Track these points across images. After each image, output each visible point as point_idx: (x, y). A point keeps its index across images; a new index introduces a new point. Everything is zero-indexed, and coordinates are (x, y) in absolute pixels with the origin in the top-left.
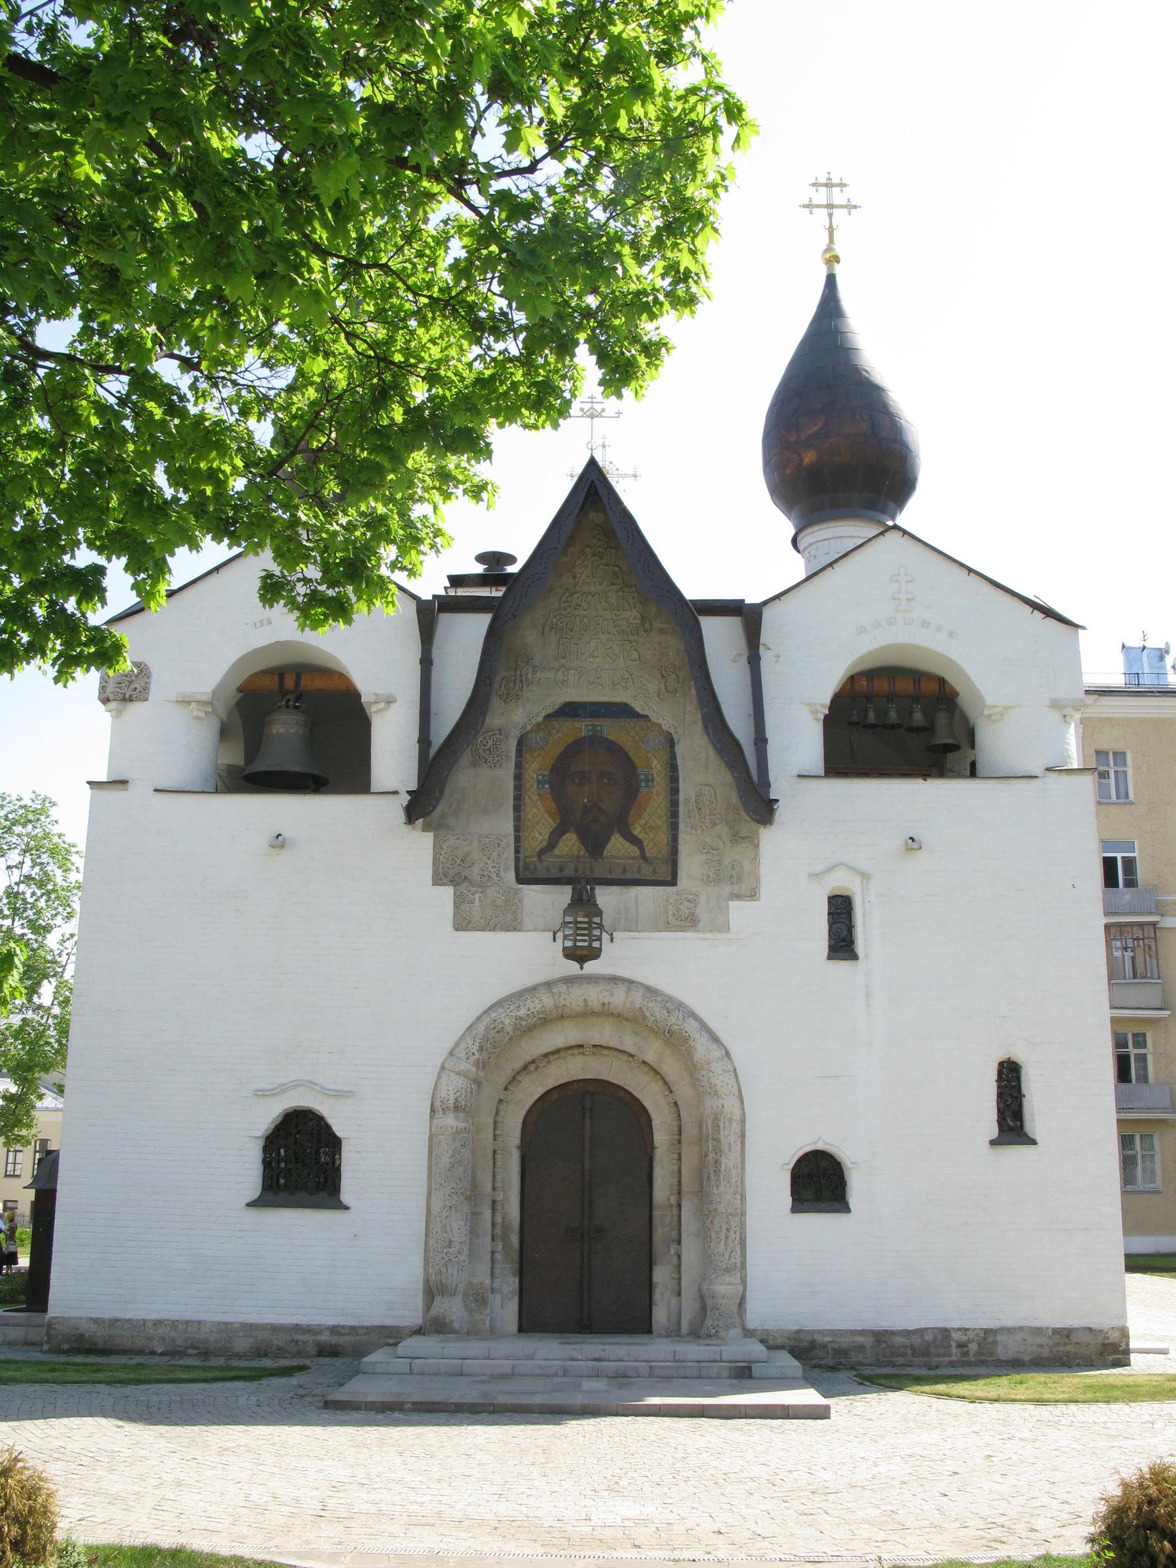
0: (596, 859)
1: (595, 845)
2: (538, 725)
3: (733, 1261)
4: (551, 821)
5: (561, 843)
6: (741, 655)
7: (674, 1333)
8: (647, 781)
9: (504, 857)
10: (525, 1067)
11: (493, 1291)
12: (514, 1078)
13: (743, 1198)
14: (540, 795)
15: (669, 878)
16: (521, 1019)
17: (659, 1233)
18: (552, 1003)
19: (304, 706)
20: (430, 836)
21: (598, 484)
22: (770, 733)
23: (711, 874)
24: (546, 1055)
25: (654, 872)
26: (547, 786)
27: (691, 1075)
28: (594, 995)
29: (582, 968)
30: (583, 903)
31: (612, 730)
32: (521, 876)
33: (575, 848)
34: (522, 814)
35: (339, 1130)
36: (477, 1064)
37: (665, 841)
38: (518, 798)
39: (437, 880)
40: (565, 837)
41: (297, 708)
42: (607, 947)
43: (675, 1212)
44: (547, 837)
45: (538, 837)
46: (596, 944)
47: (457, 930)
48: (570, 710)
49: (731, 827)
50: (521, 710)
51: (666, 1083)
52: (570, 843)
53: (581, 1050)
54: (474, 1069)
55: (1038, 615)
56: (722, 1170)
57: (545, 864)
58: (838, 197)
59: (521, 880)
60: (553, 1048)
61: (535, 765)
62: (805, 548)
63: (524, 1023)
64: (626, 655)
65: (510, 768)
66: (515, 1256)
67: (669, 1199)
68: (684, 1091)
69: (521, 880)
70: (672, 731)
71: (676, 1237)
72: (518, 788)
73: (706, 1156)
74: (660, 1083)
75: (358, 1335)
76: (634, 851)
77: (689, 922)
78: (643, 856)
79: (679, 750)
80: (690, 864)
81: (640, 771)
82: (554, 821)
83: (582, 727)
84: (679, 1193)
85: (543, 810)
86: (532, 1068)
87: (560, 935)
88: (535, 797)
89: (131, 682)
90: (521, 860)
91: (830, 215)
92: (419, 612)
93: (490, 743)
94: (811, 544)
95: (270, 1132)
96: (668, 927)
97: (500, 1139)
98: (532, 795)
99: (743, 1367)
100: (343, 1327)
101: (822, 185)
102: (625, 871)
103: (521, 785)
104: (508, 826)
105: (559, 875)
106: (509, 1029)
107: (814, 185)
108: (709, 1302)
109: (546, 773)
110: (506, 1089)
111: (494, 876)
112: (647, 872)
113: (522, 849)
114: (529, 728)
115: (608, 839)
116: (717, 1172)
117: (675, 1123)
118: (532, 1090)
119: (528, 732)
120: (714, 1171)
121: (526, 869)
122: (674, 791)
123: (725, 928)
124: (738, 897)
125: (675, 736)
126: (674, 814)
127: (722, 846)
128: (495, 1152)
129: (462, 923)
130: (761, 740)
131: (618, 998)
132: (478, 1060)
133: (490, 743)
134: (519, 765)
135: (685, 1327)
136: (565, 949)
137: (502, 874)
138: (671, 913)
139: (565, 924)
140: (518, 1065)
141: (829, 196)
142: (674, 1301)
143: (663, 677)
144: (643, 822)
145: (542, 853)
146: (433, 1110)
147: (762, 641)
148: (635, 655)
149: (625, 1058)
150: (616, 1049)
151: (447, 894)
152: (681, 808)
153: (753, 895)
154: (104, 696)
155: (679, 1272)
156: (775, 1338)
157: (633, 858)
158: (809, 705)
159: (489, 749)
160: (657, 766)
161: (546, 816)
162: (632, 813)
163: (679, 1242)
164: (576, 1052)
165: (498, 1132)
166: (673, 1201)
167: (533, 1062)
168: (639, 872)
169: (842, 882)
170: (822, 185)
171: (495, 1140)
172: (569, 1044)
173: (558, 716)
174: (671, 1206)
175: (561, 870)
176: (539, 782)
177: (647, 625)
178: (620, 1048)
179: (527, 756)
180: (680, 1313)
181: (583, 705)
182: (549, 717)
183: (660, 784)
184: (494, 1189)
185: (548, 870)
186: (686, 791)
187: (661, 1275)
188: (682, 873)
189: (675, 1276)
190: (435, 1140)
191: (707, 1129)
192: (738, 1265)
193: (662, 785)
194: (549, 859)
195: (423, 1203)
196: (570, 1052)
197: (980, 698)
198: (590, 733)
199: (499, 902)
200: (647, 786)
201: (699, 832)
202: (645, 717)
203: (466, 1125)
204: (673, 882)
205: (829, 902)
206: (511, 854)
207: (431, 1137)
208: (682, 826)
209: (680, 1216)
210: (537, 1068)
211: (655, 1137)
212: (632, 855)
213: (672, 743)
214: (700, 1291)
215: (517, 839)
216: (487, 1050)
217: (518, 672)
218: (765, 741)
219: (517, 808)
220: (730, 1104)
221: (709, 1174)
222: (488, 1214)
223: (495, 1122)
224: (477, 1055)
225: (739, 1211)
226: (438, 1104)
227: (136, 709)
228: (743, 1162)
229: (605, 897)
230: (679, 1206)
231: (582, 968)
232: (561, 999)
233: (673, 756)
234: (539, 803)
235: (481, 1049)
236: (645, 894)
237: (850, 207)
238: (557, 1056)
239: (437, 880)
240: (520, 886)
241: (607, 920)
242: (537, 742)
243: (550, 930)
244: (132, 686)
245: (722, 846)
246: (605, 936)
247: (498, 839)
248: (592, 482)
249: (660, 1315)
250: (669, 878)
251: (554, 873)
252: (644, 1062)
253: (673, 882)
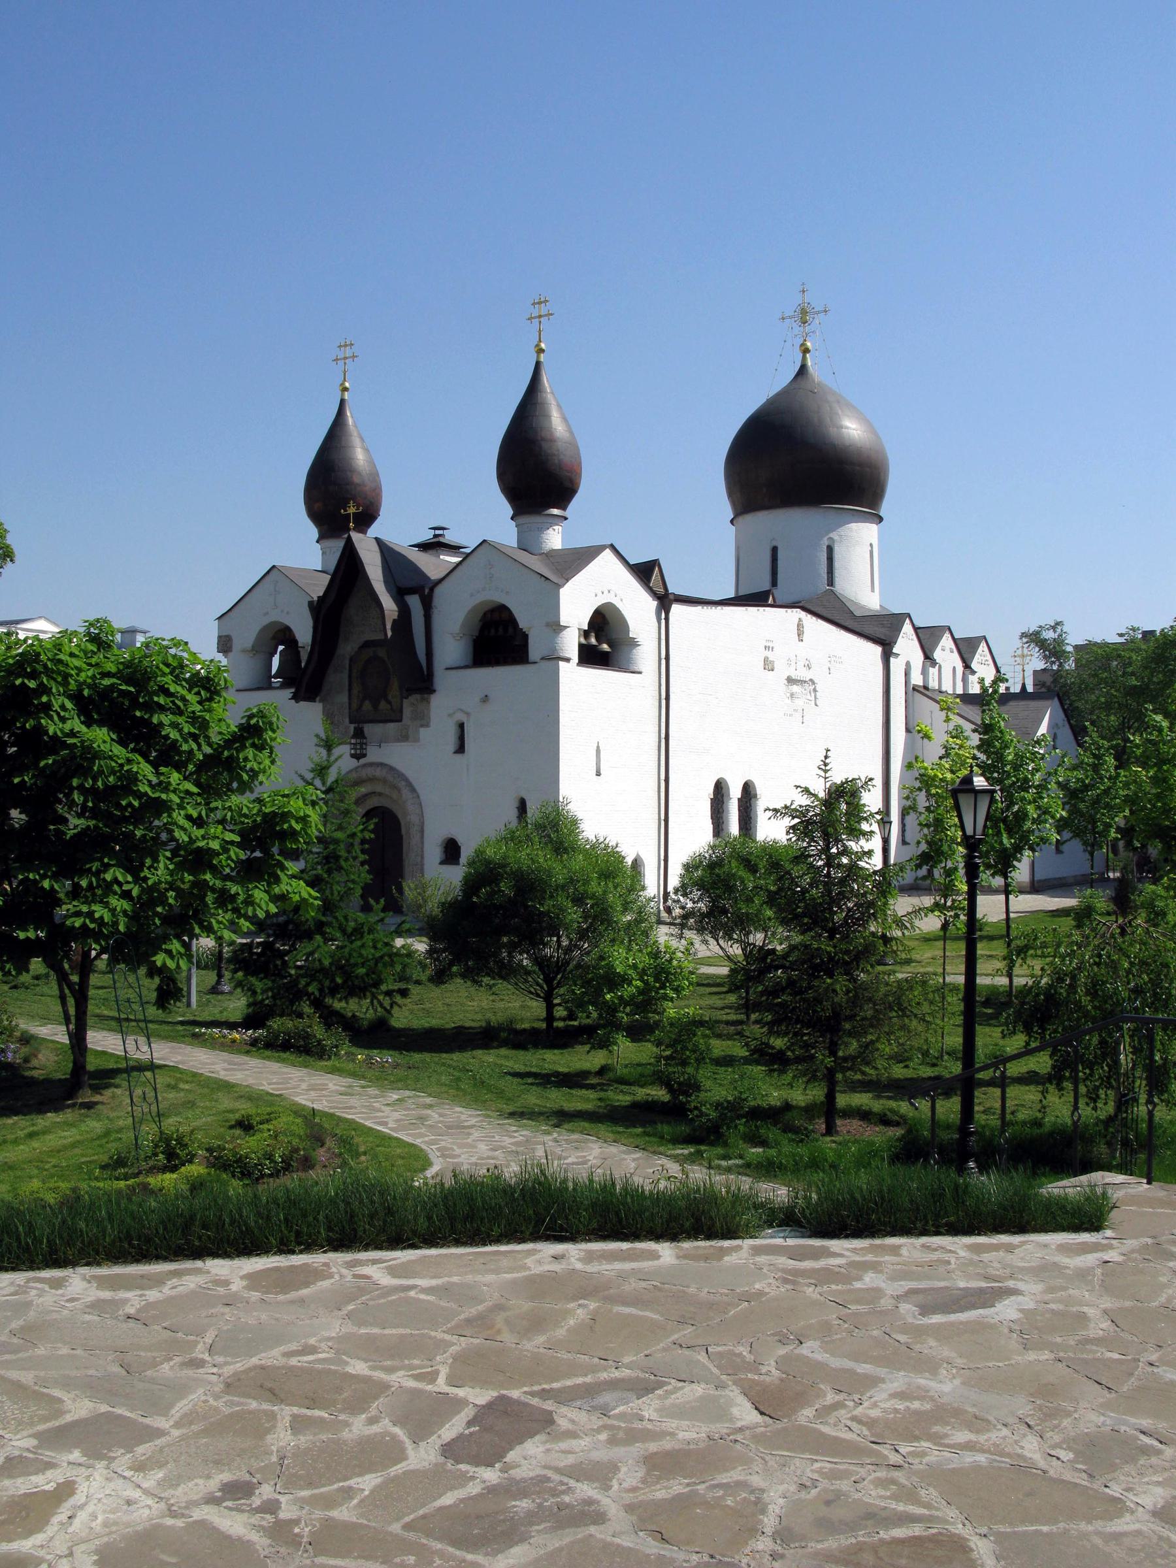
1: (375, 707)
13: (422, 857)
28: (370, 772)
30: (359, 734)
38: (350, 685)
48: (367, 645)
52: (367, 705)
65: (346, 672)
76: (389, 707)
77: (404, 737)
80: (407, 712)
96: (398, 740)
123: (417, 740)
124: (422, 726)
131: (378, 772)
134: (350, 671)
153: (427, 725)
169: (461, 717)
181: (373, 641)
204: (400, 720)
206: (347, 711)
220: (414, 818)
227: (231, 654)
228: (422, 843)
229: (368, 729)
236: (391, 727)
253: (400, 720)
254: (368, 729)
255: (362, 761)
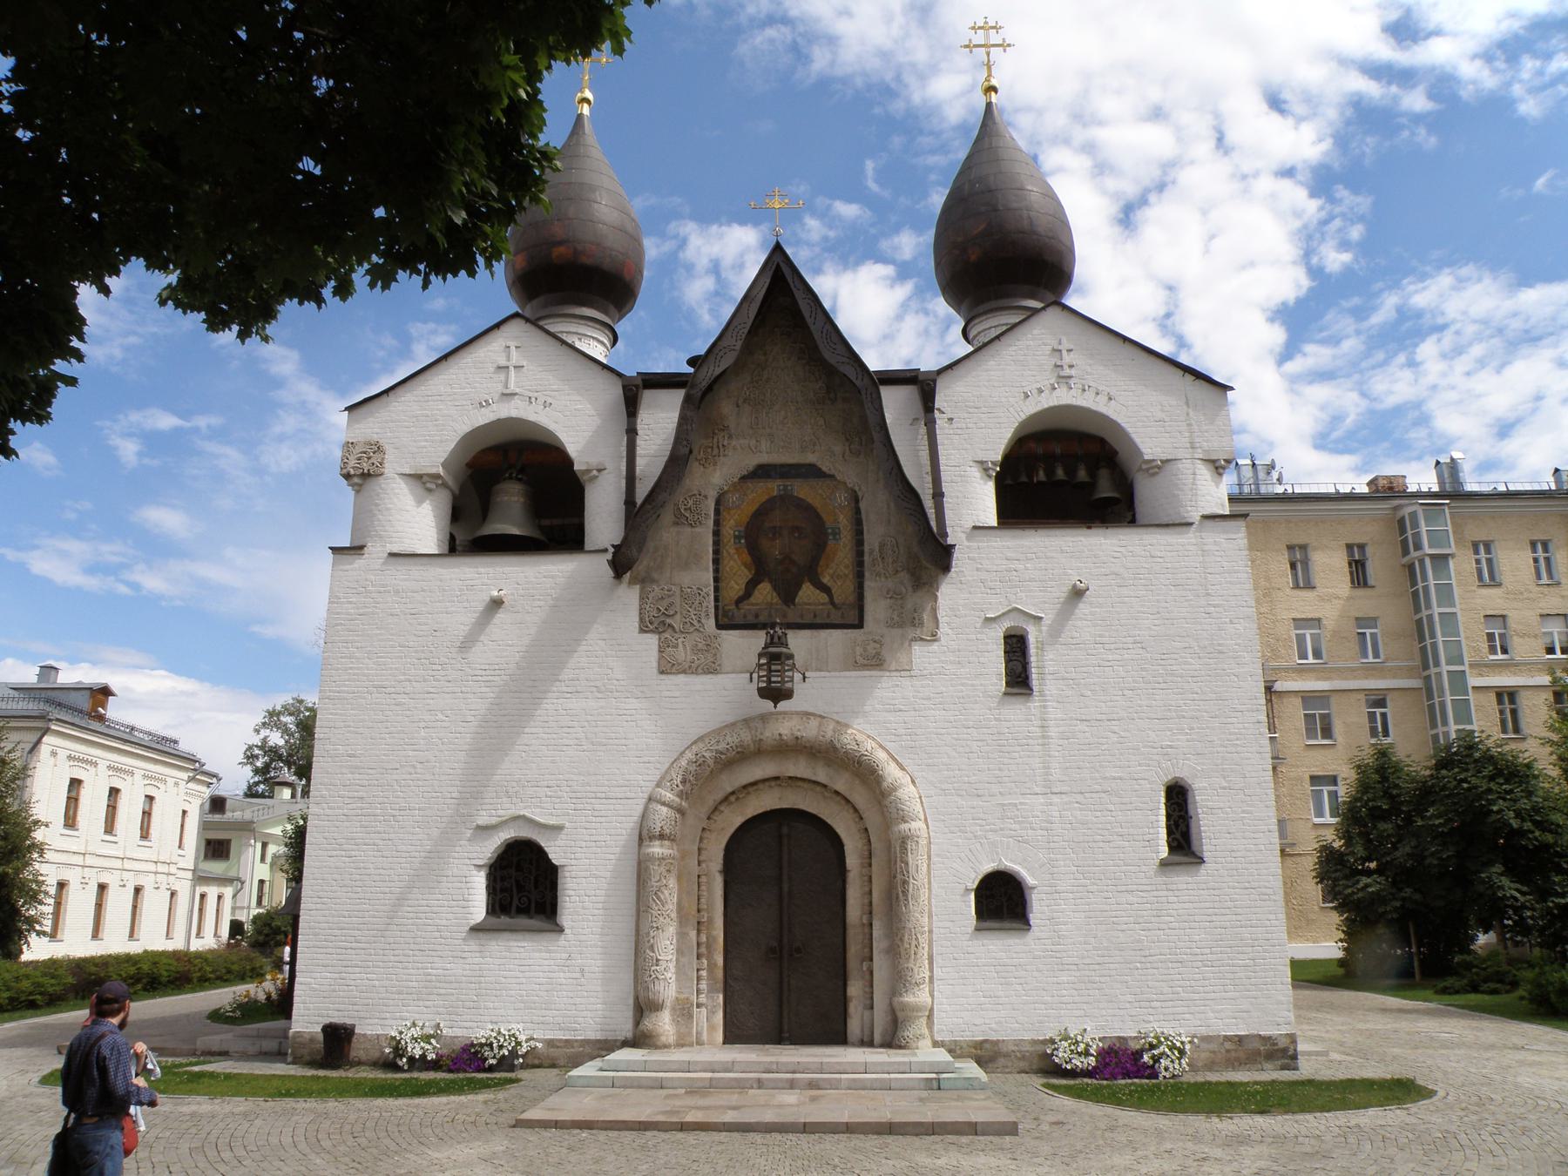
0: (789, 606)
1: (788, 596)
2: (734, 485)
3: (922, 975)
4: (746, 571)
5: (756, 592)
6: (916, 419)
7: (867, 1042)
8: (834, 534)
9: (704, 605)
10: (726, 799)
11: (698, 1006)
12: (716, 809)
14: (737, 549)
15: (856, 622)
16: (721, 753)
17: (854, 949)
18: (749, 738)
19: (525, 478)
20: (637, 588)
21: (782, 265)
22: (946, 488)
23: (895, 617)
24: (745, 787)
25: (843, 616)
26: (743, 541)
27: (880, 803)
28: (785, 729)
29: (775, 707)
31: (803, 490)
32: (720, 623)
33: (769, 596)
34: (721, 567)
35: (555, 856)
36: (680, 795)
37: (852, 588)
38: (716, 552)
39: (643, 629)
40: (759, 587)
41: (520, 480)
42: (799, 688)
43: (867, 930)
44: (743, 586)
45: (735, 587)
46: (789, 685)
47: (662, 673)
48: (763, 472)
49: (913, 574)
50: (718, 474)
51: (856, 810)
52: (765, 592)
53: (778, 782)
54: (677, 799)
55: (1189, 378)
56: (911, 890)
57: (742, 611)
58: (995, 38)
59: (720, 626)
60: (752, 780)
61: (732, 522)
62: (975, 337)
63: (723, 757)
64: (813, 421)
66: (720, 974)
67: (861, 919)
68: (872, 820)
69: (720, 626)
70: (857, 489)
71: (868, 955)
72: (716, 543)
73: (895, 877)
74: (851, 811)
75: (573, 1047)
76: (824, 598)
78: (832, 603)
79: (862, 505)
80: (876, 609)
81: (828, 524)
82: (750, 570)
83: (773, 487)
84: (871, 913)
85: (739, 563)
86: (732, 798)
87: (755, 676)
88: (732, 551)
89: (369, 458)
90: (720, 607)
91: (988, 54)
92: (624, 387)
93: (691, 502)
94: (979, 333)
95: (492, 861)
96: (856, 666)
97: (704, 865)
98: (729, 549)
99: (932, 1079)
100: (560, 1040)
101: (980, 28)
102: (815, 616)
103: (719, 541)
104: (710, 575)
105: (755, 622)
106: (711, 762)
107: (973, 28)
108: (900, 1015)
109: (742, 529)
110: (709, 818)
111: (695, 623)
112: (836, 617)
113: (720, 598)
114: (726, 488)
115: (798, 587)
116: (905, 893)
117: (865, 848)
118: (734, 819)
119: (725, 492)
120: (903, 892)
121: (723, 616)
122: (859, 542)
125: (860, 494)
126: (860, 564)
127: (904, 590)
128: (699, 876)
129: (667, 667)
130: (938, 495)
132: (682, 791)
133: (691, 502)
134: (717, 523)
135: (877, 1038)
136: (759, 690)
137: (703, 621)
138: (858, 653)
139: (760, 666)
140: (720, 796)
141: (987, 37)
142: (867, 1013)
143: (847, 440)
144: (831, 571)
145: (739, 601)
146: (641, 839)
147: (937, 405)
148: (821, 422)
149: (818, 789)
150: (810, 781)
151: (652, 640)
152: (866, 558)
154: (345, 471)
155: (872, 986)
156: (961, 1048)
157: (823, 604)
158: (981, 463)
159: (690, 509)
160: (844, 521)
161: (743, 568)
162: (821, 563)
163: (871, 960)
164: (773, 783)
165: (702, 858)
166: (865, 921)
167: (733, 793)
168: (828, 616)
170: (980, 28)
171: (699, 865)
172: (766, 777)
173: (752, 478)
174: (864, 925)
175: (757, 616)
176: (735, 537)
177: (832, 395)
178: (814, 778)
179: (724, 514)
180: (873, 1025)
182: (743, 478)
183: (846, 538)
184: (699, 911)
185: (745, 616)
186: (872, 541)
187: (854, 989)
188: (868, 617)
189: (867, 989)
190: (643, 865)
191: (895, 853)
192: (927, 979)
193: (849, 537)
194: (745, 606)
195: (633, 925)
196: (767, 784)
197: (1139, 452)
198: (782, 493)
199: (700, 646)
200: (834, 539)
201: (883, 579)
202: (832, 477)
203: (671, 851)
205: (1005, 643)
207: (639, 863)
208: (867, 574)
209: (871, 935)
210: (737, 799)
211: (848, 861)
212: (822, 601)
213: (857, 501)
214: (891, 1004)
215: (716, 589)
216: (690, 781)
217: (715, 440)
218: (942, 495)
219: (716, 561)
221: (897, 894)
222: (693, 934)
223: (699, 849)
224: (681, 787)
225: (926, 929)
226: (645, 832)
230: (871, 925)
231: (775, 707)
232: (758, 734)
233: (858, 511)
234: (736, 556)
235: (684, 782)
236: (835, 639)
237: (1004, 46)
238: (755, 787)
239: (643, 629)
240: (719, 631)
241: (799, 660)
242: (733, 502)
243: (747, 672)
244: (370, 462)
245: (904, 590)
246: (798, 676)
247: (698, 589)
248: (778, 265)
249: (854, 1027)
250: (856, 622)
251: (751, 619)
252: (837, 793)
254: (799, 642)
255: (783, 705)
